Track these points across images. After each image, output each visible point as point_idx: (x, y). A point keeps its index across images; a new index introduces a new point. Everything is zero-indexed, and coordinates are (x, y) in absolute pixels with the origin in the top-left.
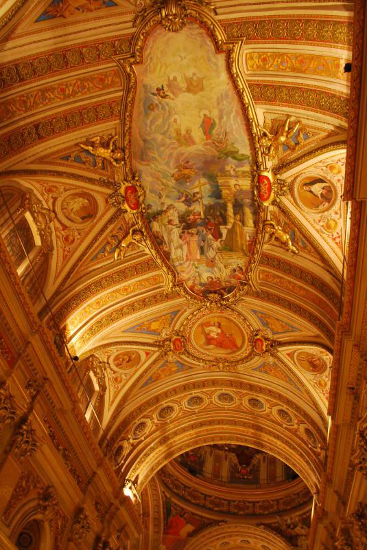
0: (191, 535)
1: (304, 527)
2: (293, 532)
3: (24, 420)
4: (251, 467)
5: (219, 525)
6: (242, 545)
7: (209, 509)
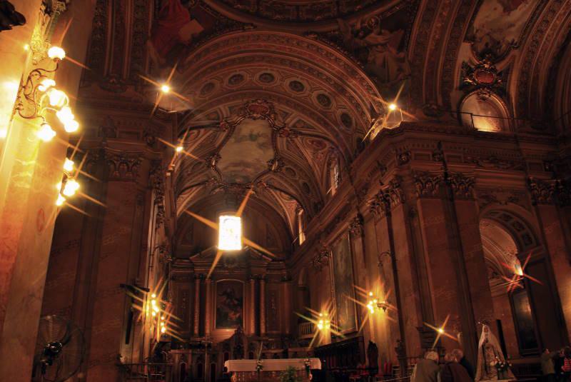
0: (198, 39)
1: (383, 31)
5: (244, 30)
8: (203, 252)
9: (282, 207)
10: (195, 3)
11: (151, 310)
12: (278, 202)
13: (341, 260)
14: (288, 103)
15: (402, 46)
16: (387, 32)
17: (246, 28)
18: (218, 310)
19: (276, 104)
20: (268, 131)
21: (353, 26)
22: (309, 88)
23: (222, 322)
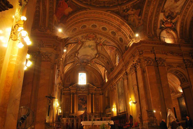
0: (70, 14)
1: (133, 10)
2: (126, 13)
5: (86, 10)
9: (100, 70)
10: (70, 2)
11: (56, 105)
12: (98, 68)
13: (120, 88)
14: (101, 34)
15: (140, 15)
16: (135, 10)
17: (87, 9)
18: (78, 105)
19: (97, 35)
20: (95, 44)
21: (123, 8)
22: (108, 30)
23: (80, 109)
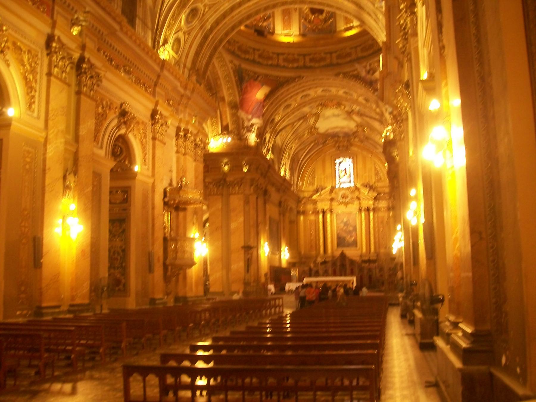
0: (267, 97)
3: (82, 59)
4: (324, 15)
6: (323, 94)
7: (284, 67)
8: (322, 192)
